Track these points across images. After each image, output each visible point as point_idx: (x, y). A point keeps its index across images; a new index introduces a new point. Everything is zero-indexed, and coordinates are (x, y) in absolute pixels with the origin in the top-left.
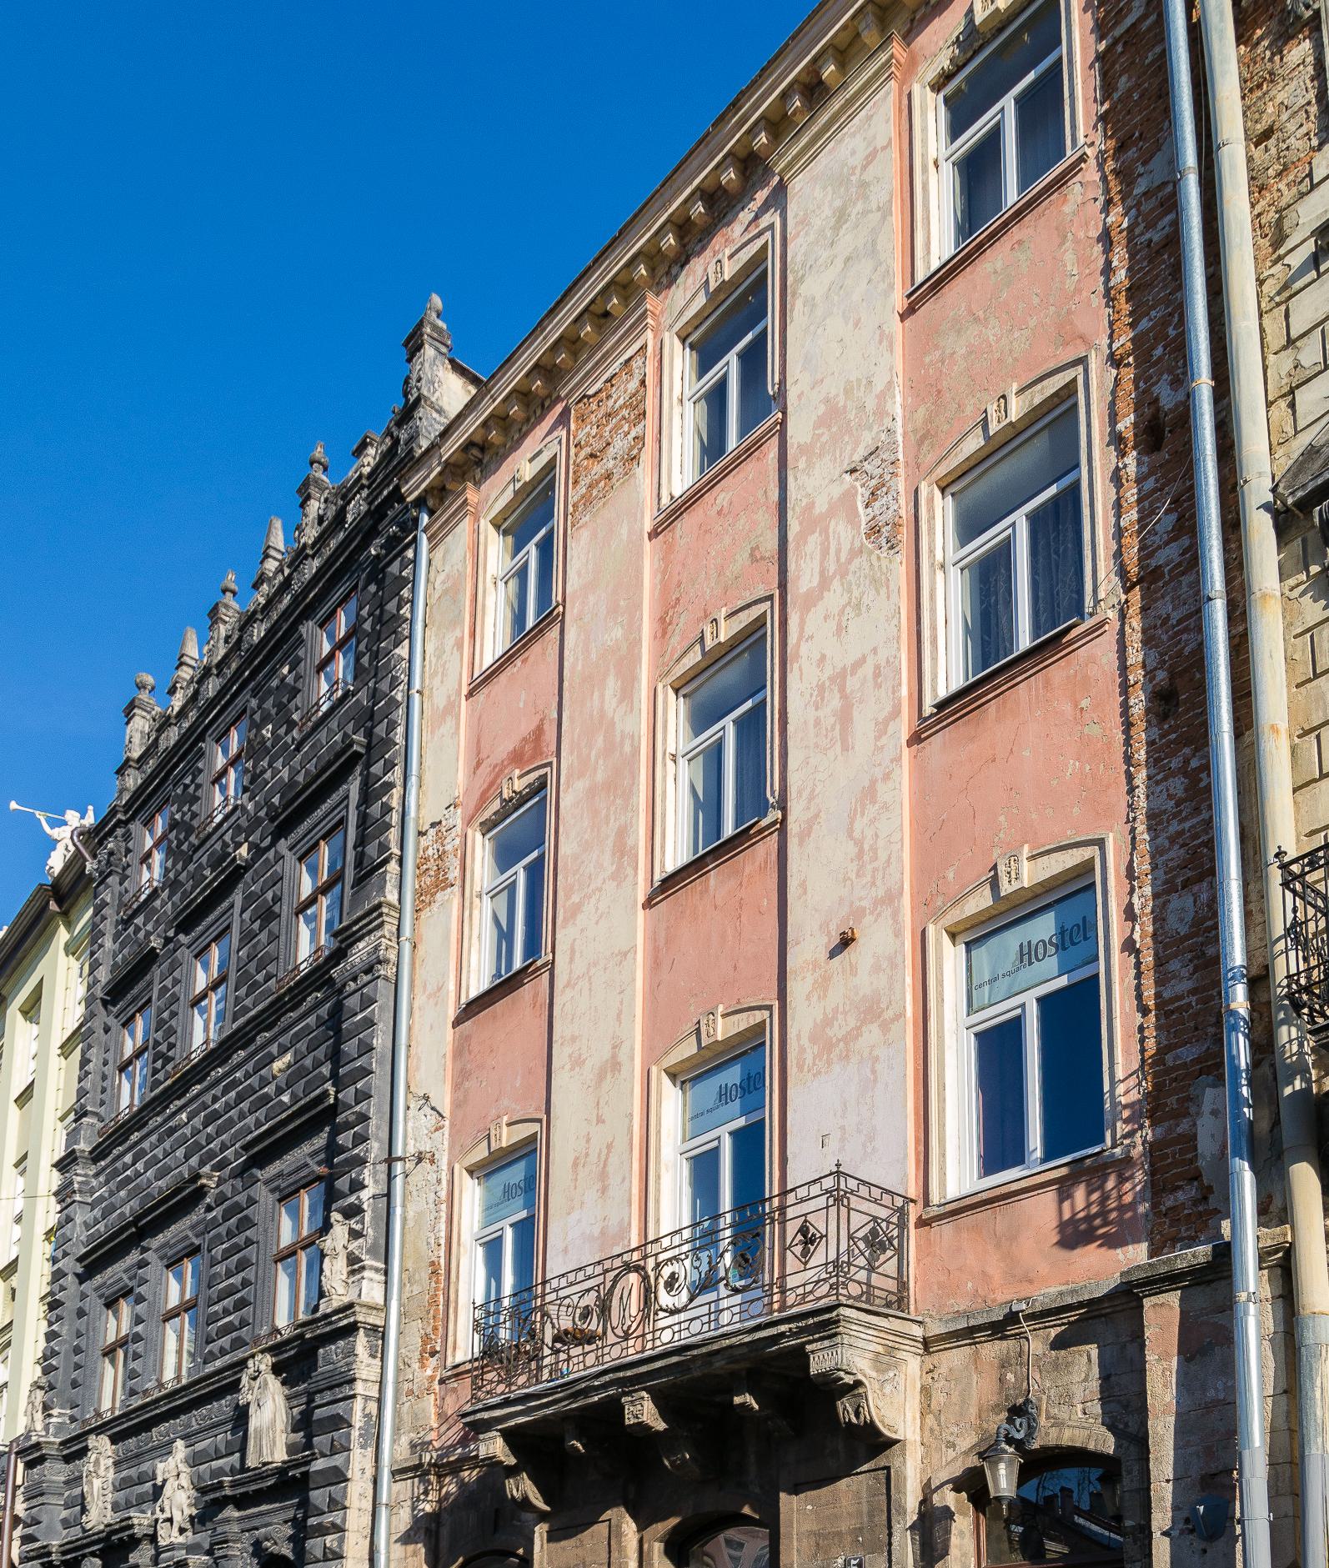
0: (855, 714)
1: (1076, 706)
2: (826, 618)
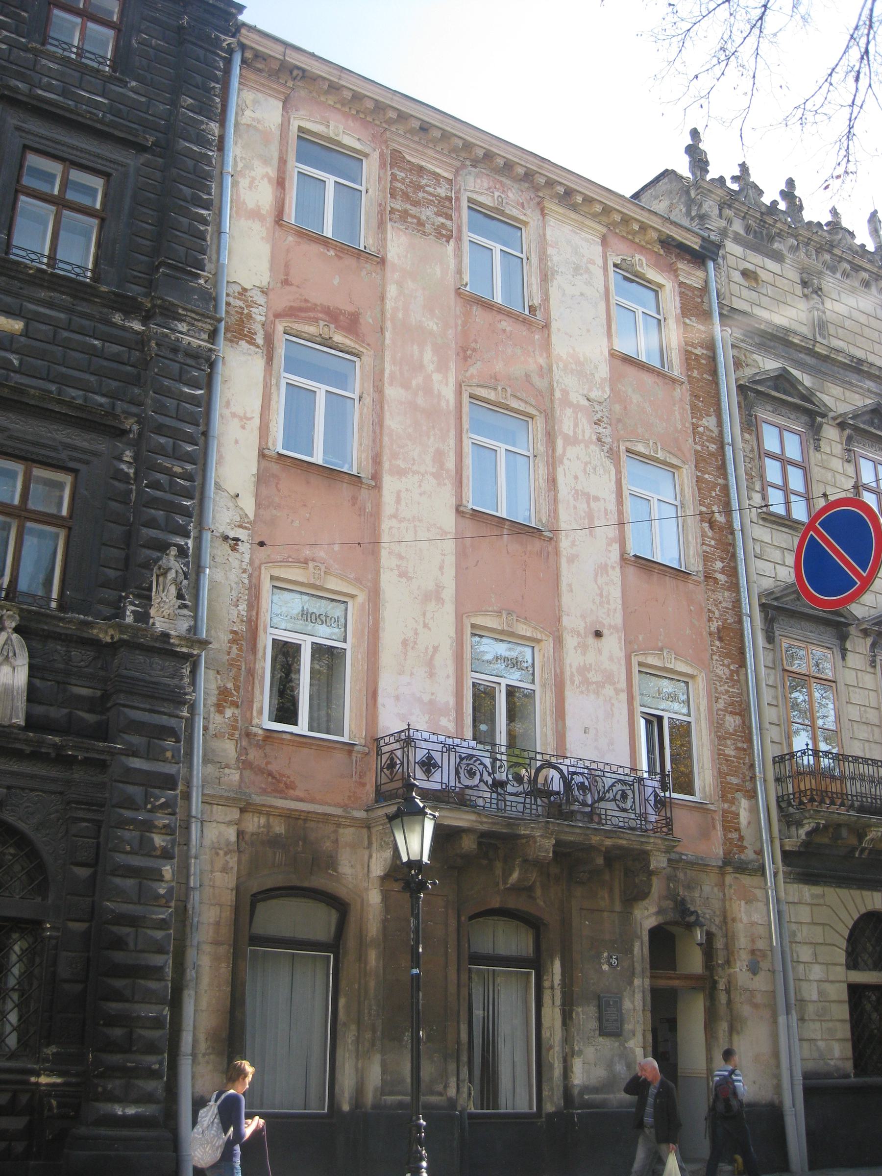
1: (689, 606)
2: (578, 458)
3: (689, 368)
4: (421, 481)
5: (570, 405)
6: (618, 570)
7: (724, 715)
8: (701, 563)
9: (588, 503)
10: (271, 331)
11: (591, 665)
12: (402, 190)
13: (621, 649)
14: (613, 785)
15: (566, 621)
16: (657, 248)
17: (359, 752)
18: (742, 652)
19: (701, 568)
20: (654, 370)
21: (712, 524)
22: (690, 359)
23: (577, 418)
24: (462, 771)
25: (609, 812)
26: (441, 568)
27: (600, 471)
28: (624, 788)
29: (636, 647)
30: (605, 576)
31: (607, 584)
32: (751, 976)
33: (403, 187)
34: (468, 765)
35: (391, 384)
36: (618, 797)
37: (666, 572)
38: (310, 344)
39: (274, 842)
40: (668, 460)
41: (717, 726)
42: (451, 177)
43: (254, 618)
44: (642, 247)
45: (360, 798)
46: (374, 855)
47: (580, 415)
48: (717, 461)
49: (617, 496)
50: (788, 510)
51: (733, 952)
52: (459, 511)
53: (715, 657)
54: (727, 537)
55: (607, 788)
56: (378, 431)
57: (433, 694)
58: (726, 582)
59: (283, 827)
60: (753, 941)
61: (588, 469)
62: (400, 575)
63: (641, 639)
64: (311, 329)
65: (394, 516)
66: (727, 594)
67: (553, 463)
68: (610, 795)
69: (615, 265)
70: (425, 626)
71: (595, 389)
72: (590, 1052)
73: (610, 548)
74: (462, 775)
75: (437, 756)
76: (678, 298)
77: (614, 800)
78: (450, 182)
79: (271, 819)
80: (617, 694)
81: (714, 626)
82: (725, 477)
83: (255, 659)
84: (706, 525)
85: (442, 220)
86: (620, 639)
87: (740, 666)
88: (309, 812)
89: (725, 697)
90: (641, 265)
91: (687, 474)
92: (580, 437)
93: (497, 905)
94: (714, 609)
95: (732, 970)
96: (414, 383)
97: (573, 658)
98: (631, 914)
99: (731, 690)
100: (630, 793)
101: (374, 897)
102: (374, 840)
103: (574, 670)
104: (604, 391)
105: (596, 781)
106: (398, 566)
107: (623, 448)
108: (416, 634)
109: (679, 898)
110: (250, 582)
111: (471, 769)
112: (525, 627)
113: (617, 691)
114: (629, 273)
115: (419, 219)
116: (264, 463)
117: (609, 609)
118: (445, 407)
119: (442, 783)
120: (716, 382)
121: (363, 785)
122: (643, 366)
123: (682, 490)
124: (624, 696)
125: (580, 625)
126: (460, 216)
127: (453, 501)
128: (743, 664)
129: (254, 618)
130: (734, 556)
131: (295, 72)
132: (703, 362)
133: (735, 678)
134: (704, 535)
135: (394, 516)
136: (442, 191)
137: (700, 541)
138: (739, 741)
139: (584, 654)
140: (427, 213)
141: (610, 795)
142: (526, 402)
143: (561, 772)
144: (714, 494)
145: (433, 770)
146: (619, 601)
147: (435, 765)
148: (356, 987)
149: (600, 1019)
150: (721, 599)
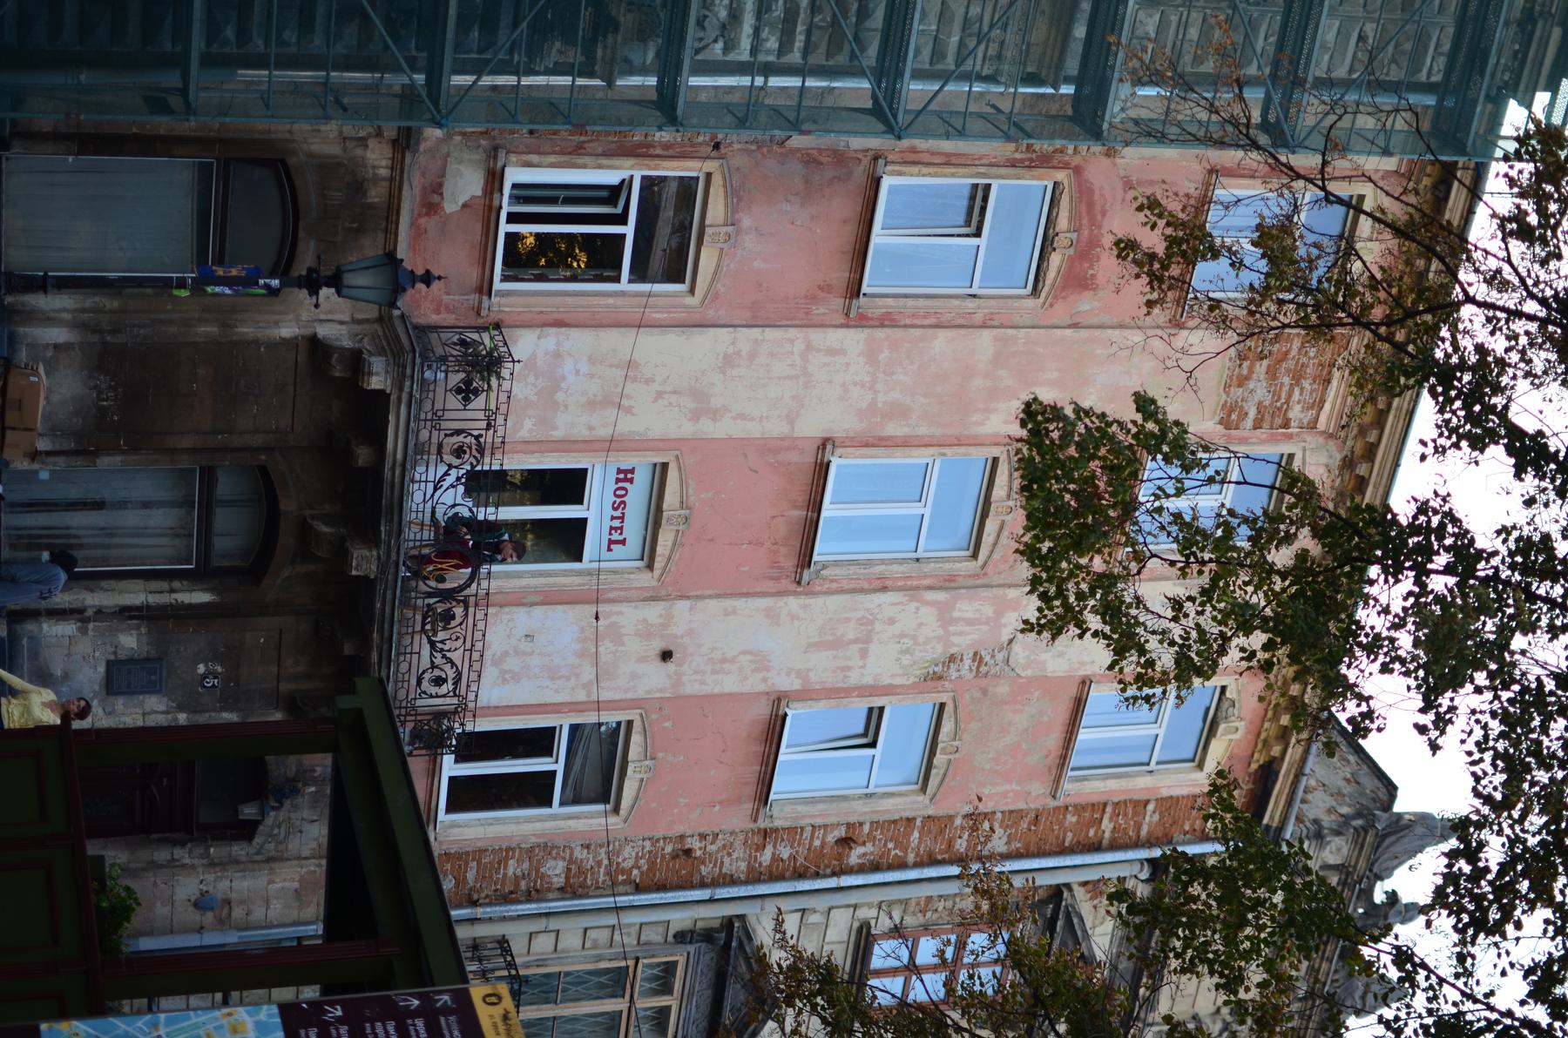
0: (829, 653)
2: (921, 625)
3: (1080, 809)
4: (863, 386)
5: (999, 614)
6: (762, 688)
7: (564, 859)
8: (786, 824)
9: (856, 641)
10: (1055, 163)
11: (623, 644)
12: (1287, 353)
13: (648, 692)
14: (453, 664)
15: (683, 605)
16: (1260, 759)
17: (480, 303)
18: (662, 887)
19: (778, 823)
20: (1067, 749)
21: (846, 842)
22: (1093, 810)
23: (981, 623)
24: (461, 438)
25: (415, 657)
26: (742, 416)
27: (906, 660)
28: (450, 682)
29: (654, 716)
30: (753, 666)
31: (741, 669)
32: (193, 899)
33: (1294, 352)
34: (470, 448)
35: (996, 339)
36: (437, 673)
37: (767, 766)
38: (1043, 220)
39: (357, 187)
40: (934, 771)
41: (546, 849)
42: (1321, 425)
43: (652, 151)
44: (1259, 734)
45: (419, 306)
46: (344, 327)
47: (985, 628)
48: (941, 851)
49: (872, 687)
50: (879, 973)
51: (226, 870)
52: (824, 444)
53: (647, 843)
54: (827, 866)
55: (448, 654)
56: (927, 322)
57: (566, 407)
58: (760, 864)
59: (376, 200)
60: (242, 902)
61: (906, 640)
62: (726, 356)
63: (666, 724)
64: (1063, 223)
65: (809, 347)
66: (743, 866)
67: (911, 589)
68: (438, 660)
69: (1224, 689)
70: (659, 395)
71: (1027, 653)
72: (85, 646)
73: (793, 675)
74: (455, 439)
75: (478, 403)
76: (1184, 791)
77: (433, 666)
78: (1313, 425)
79: (386, 184)
80: (584, 686)
81: (694, 844)
82: (919, 865)
83: (597, 155)
84: (841, 832)
85: (1252, 413)
86: (661, 690)
87: (637, 885)
88: (396, 235)
89: (591, 862)
90: (1227, 732)
91: (918, 806)
92: (951, 628)
93: (282, 507)
94: (719, 843)
95: (200, 870)
96: (1003, 373)
97: (628, 617)
98: (276, 708)
99: (602, 870)
100: (444, 689)
101: (287, 331)
102: (365, 326)
103: (613, 619)
104: (1025, 668)
105: (458, 638)
106: (738, 353)
107: (944, 698)
108: (649, 381)
109: (300, 785)
110: (701, 144)
111: (465, 452)
112: (670, 544)
113: (586, 686)
114: (1215, 714)
115: (1247, 378)
116: (865, 161)
117: (704, 673)
118: (974, 419)
119: (444, 410)
120: (1063, 851)
121: (437, 311)
122: (1071, 733)
123: (892, 795)
124: (581, 696)
125: (678, 629)
126: (1262, 442)
127: (838, 434)
128: (639, 889)
129: (652, 151)
130: (801, 875)
131: (1442, 187)
132: (1092, 833)
133: (620, 878)
134: (826, 827)
135: (809, 347)
136: (1296, 413)
137: (818, 821)
138: (527, 885)
139: (637, 634)
140: (1259, 390)
141: (438, 660)
142: (995, 544)
143: (467, 585)
144: (890, 845)
145: (460, 397)
146: (717, 690)
147: (467, 400)
148: (169, 307)
149: (130, 661)
150: (735, 855)
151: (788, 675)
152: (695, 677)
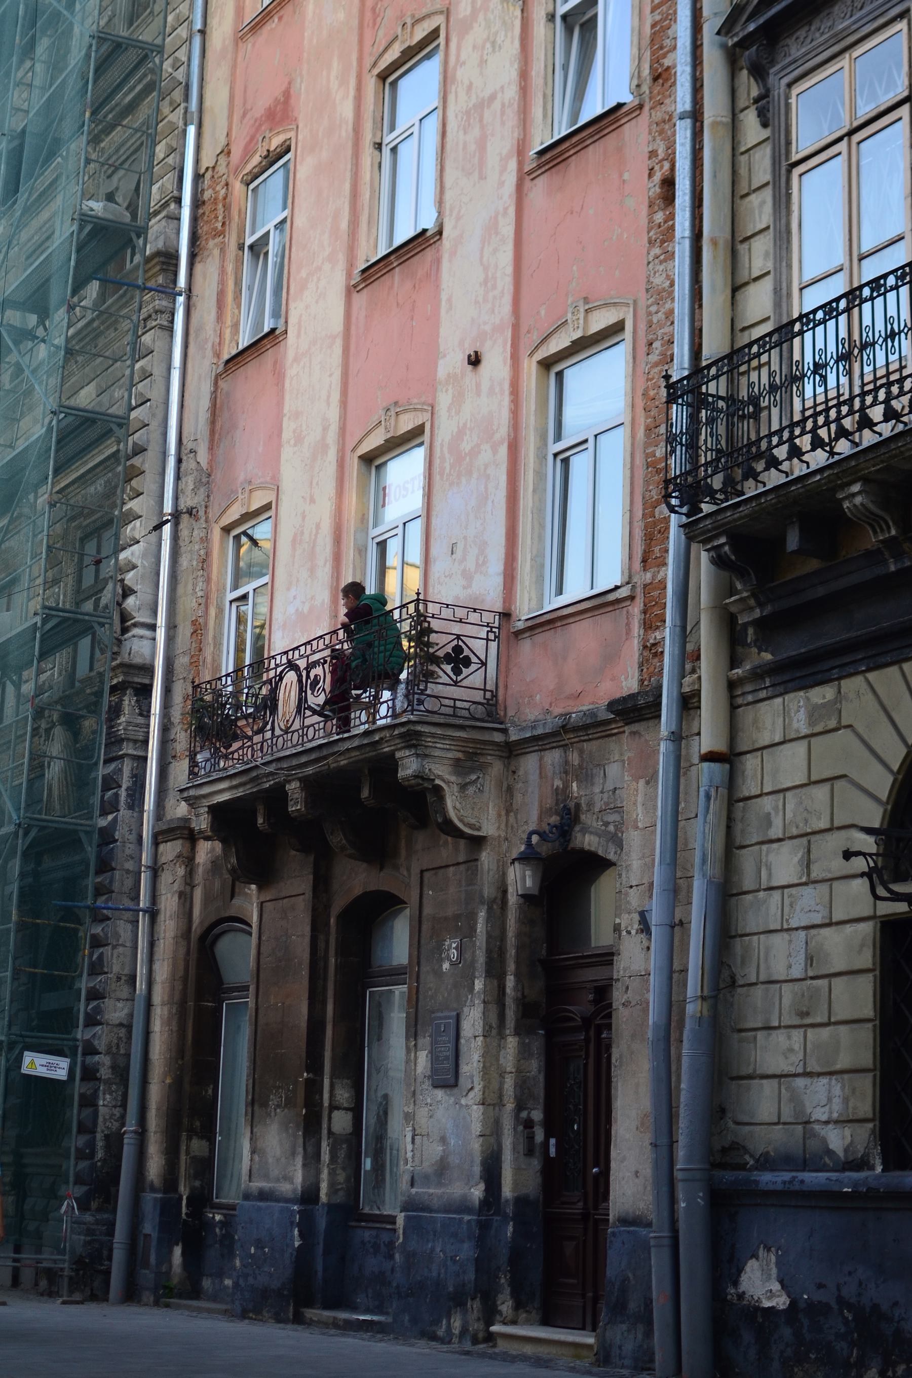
0: (489, 144)
4: (319, 279)
11: (465, 424)
106: (294, 431)
151: (503, 182)
152: (496, 311)
